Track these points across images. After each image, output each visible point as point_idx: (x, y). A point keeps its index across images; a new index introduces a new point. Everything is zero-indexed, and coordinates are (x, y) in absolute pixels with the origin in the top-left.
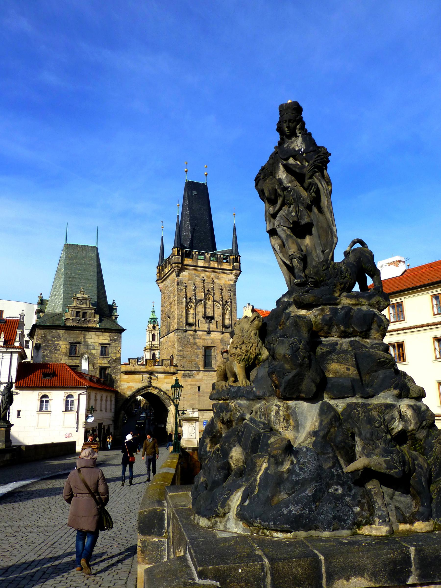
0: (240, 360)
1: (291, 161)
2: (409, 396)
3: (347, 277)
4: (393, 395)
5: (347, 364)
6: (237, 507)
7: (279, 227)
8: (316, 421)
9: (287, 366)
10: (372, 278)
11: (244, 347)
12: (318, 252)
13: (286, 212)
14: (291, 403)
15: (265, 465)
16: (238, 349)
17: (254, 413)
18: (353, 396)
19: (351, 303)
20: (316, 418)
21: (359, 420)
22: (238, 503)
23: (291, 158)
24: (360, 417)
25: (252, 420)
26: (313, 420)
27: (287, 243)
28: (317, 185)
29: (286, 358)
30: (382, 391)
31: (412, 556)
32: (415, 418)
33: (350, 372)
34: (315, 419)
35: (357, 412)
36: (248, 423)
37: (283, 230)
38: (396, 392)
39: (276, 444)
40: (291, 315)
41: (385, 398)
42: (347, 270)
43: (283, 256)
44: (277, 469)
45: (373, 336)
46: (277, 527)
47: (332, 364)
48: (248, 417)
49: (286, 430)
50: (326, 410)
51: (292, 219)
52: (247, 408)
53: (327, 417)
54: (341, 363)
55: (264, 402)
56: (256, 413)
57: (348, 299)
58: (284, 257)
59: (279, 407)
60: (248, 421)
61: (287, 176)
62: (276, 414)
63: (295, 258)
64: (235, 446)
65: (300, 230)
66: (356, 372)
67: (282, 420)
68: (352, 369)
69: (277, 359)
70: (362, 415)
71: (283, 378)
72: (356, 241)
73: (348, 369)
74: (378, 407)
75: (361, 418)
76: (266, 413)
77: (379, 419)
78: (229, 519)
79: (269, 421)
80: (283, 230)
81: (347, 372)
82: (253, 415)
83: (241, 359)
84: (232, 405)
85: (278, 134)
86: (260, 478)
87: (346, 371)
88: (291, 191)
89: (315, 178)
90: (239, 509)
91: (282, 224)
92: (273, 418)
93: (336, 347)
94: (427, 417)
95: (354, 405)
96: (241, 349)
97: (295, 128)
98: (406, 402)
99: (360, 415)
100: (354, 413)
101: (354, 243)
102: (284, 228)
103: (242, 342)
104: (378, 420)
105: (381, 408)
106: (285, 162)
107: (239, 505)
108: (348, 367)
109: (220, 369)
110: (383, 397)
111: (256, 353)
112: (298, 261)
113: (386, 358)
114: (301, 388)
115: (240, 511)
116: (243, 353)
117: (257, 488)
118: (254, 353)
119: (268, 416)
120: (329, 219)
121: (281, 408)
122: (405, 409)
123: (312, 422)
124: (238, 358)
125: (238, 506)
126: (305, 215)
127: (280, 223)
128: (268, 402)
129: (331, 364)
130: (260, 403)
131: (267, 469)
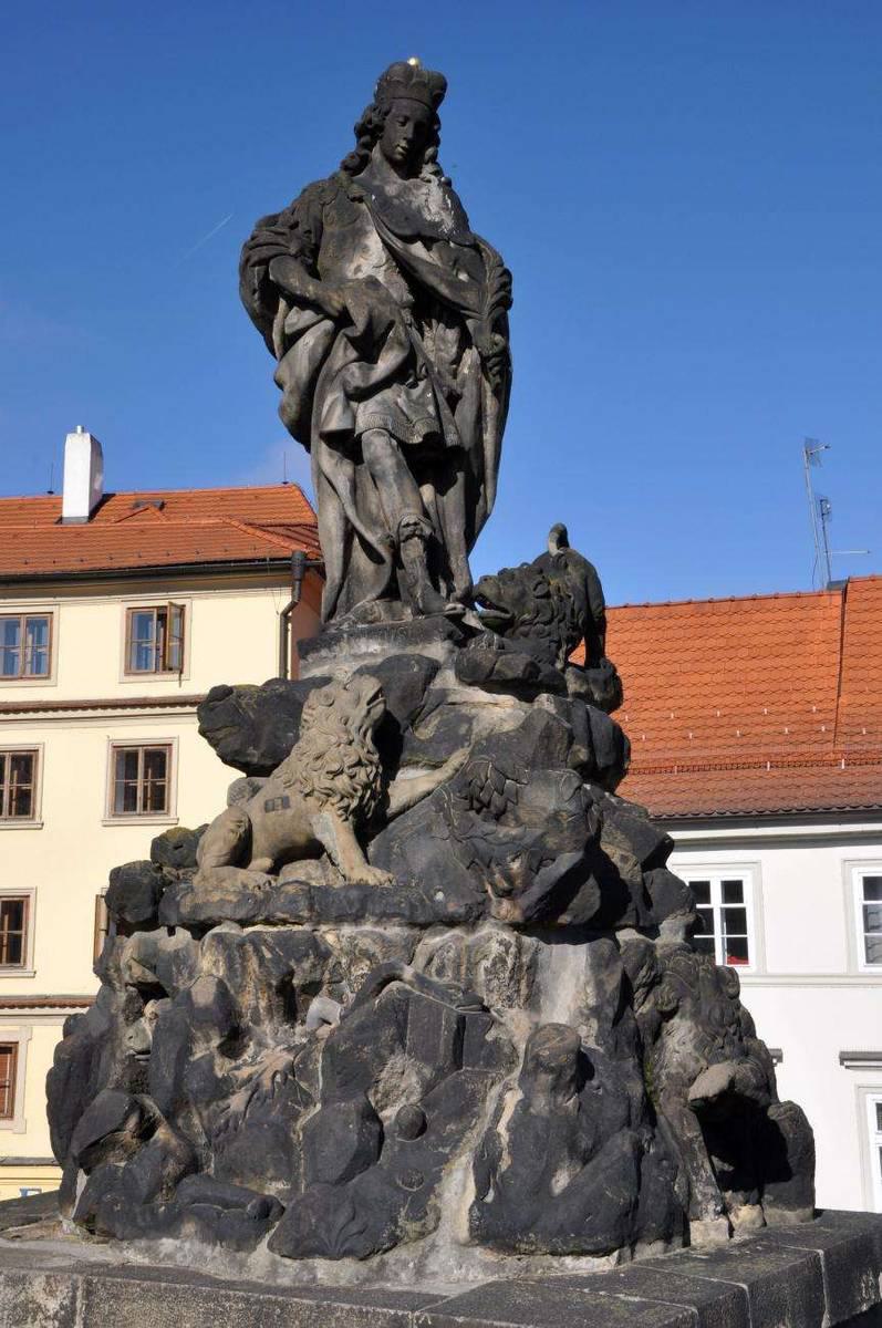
0: (346, 809)
6: (471, 1210)
8: (587, 983)
15: (512, 1099)
16: (344, 778)
17: (420, 961)
20: (586, 976)
21: (698, 978)
22: (471, 1196)
25: (421, 981)
26: (578, 979)
31: (822, 1263)
34: (582, 978)
36: (408, 987)
39: (549, 1040)
40: (450, 700)
44: (555, 1102)
46: (585, 1241)
49: (511, 1006)
58: (362, 522)
60: (410, 983)
62: (494, 964)
64: (392, 1052)
71: (537, 873)
78: (433, 1246)
79: (470, 984)
84: (330, 936)
86: (508, 1129)
90: (476, 1213)
92: (482, 976)
106: (398, 244)
107: (474, 1202)
115: (479, 1219)
116: (356, 790)
117: (505, 1155)
119: (468, 969)
125: (472, 1206)
130: (441, 933)
131: (525, 1105)
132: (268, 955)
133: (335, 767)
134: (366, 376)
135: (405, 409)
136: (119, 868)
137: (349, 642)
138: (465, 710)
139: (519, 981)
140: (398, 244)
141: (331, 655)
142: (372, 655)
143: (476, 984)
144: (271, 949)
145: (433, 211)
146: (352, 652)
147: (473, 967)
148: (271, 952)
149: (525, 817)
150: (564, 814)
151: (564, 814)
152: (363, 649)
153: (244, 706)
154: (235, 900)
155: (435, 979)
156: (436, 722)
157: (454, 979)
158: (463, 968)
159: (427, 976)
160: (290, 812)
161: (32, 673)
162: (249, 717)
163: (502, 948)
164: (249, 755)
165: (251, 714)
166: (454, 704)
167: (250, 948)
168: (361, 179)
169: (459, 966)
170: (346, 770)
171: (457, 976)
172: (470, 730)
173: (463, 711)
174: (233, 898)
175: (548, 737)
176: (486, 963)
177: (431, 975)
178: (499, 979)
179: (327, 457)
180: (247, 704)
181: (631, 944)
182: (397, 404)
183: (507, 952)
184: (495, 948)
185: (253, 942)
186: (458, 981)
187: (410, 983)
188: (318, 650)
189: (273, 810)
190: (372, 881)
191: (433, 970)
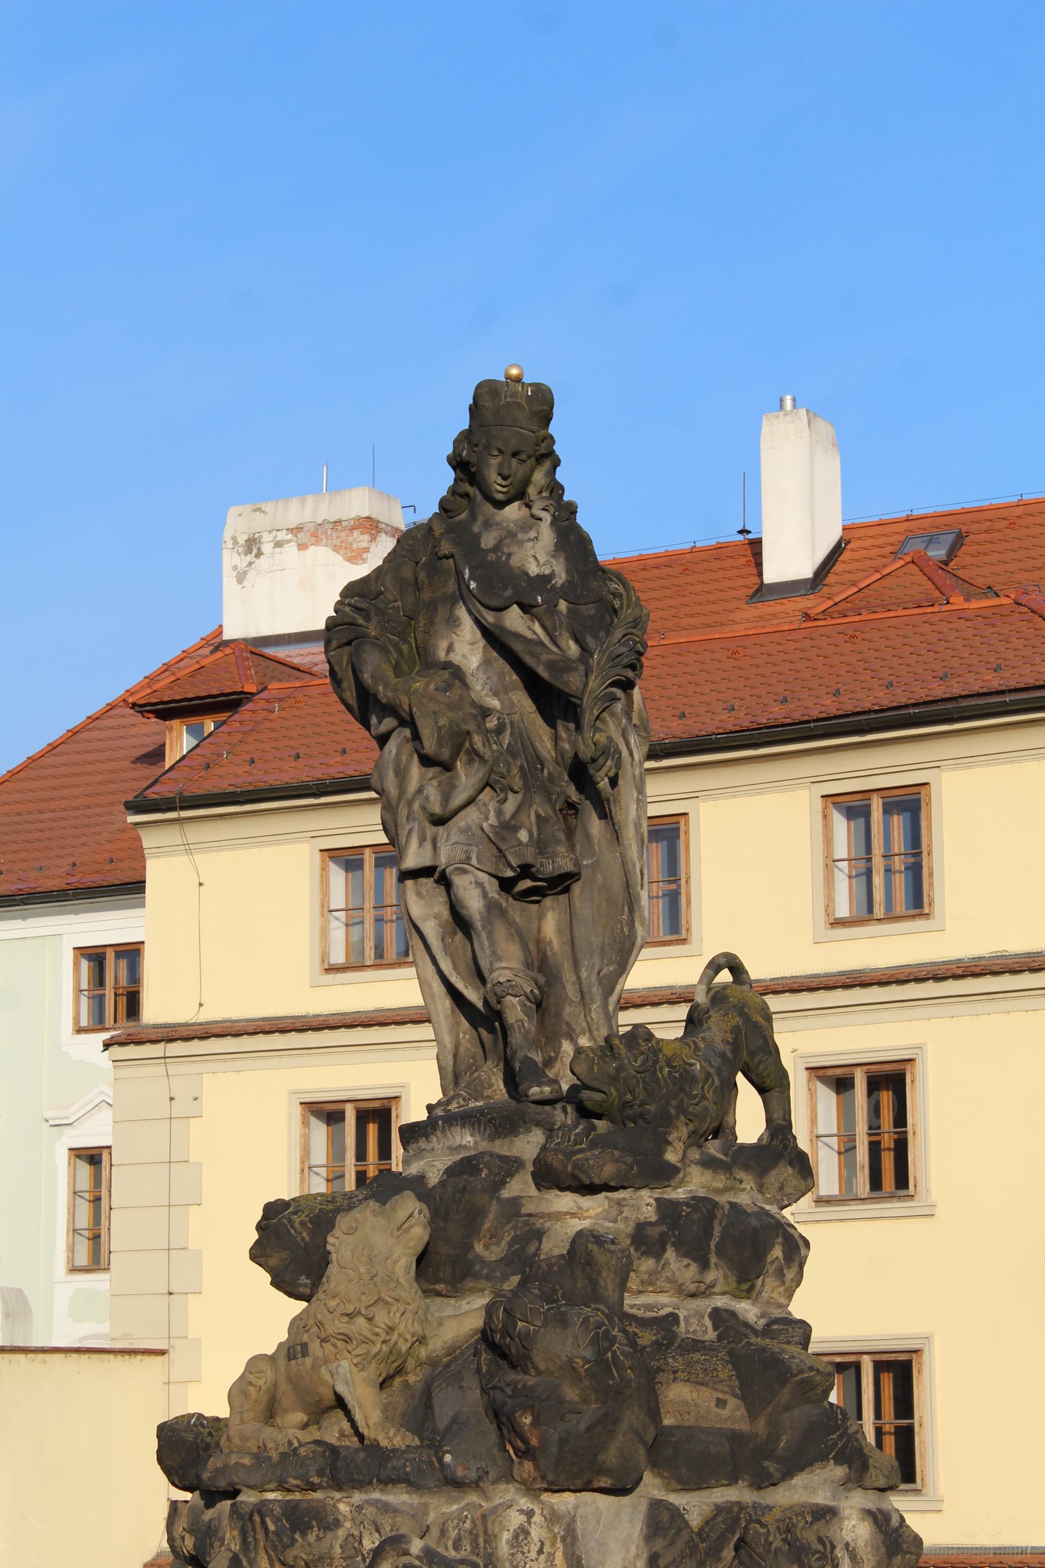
1: (514, 619)
2: (867, 1483)
3: (706, 1098)
4: (832, 1482)
5: (719, 1386)
7: (465, 872)
8: (637, 1557)
9: (571, 1393)
10: (762, 1090)
11: (382, 1318)
12: (584, 974)
13: (493, 820)
14: (565, 1501)
16: (361, 1321)
17: (435, 1533)
18: (733, 1481)
19: (715, 1184)
20: (638, 1547)
21: (769, 1551)
23: (515, 606)
24: (771, 1543)
26: (628, 1551)
27: (490, 936)
28: (620, 753)
29: (574, 1369)
30: (802, 1470)
32: (878, 1548)
33: (725, 1413)
34: (633, 1548)
35: (763, 1531)
36: (417, 1563)
37: (480, 885)
38: (841, 1472)
40: (523, 1211)
41: (813, 1486)
42: (708, 1075)
43: (455, 968)
45: (765, 1295)
47: (674, 1386)
48: (416, 1546)
50: (661, 1522)
51: (518, 855)
52: (413, 1516)
53: (672, 1543)
54: (702, 1384)
55: (474, 1498)
56: (443, 1533)
57: (706, 1172)
59: (530, 1514)
61: (486, 663)
62: (516, 1536)
63: (516, 996)
65: (530, 884)
66: (741, 1412)
67: (533, 1555)
68: (732, 1402)
69: (535, 1368)
70: (775, 1538)
72: (723, 961)
73: (721, 1403)
74: (796, 1515)
75: (773, 1546)
76: (482, 1533)
77: (820, 1547)
80: (480, 885)
81: (718, 1410)
82: (431, 1540)
83: (366, 1354)
85: (448, 476)
87: (715, 1409)
88: (499, 730)
89: (611, 723)
91: (474, 861)
93: (675, 1328)
94: (904, 1546)
95: (736, 1509)
96: (370, 1320)
97: (527, 481)
98: (856, 1499)
99: (771, 1539)
100: (756, 1532)
101: (714, 966)
102: (481, 874)
103: (376, 1298)
104: (817, 1552)
105: (804, 1517)
106: (490, 617)
108: (721, 1396)
109: (261, 1383)
110: (805, 1487)
111: (413, 1335)
112: (523, 1005)
113: (818, 1370)
114: (601, 1457)
116: (377, 1335)
118: (408, 1337)
119: (486, 1541)
120: (634, 866)
121: (537, 1518)
122: (853, 1522)
123: (624, 1559)
124: (359, 1351)
126: (558, 842)
127: (469, 858)
128: (487, 1498)
129: (668, 1385)
132: (272, 1527)
133: (350, 1309)
134: (446, 798)
135: (491, 835)
136: (165, 1423)
137: (443, 1131)
138: (538, 1223)
139: (551, 1556)
140: (490, 617)
141: (429, 1147)
142: (465, 1147)
143: (498, 1560)
144: (277, 1520)
145: (542, 561)
146: (448, 1144)
147: (490, 1539)
148: (276, 1525)
149: (542, 1366)
150: (578, 1360)
151: (579, 1361)
152: (458, 1141)
153: (297, 1225)
154: (249, 1464)
155: (452, 1554)
156: (508, 1239)
157: (472, 1552)
158: (481, 1540)
159: (441, 1550)
160: (308, 1361)
161: (665, 934)
162: (303, 1239)
163: (523, 1518)
164: (300, 1285)
165: (305, 1234)
166: (530, 1215)
167: (257, 1518)
168: (461, 521)
169: (477, 1537)
170: (363, 1312)
171: (475, 1546)
172: (538, 1249)
173: (538, 1225)
174: (247, 1461)
175: (589, 1265)
176: (506, 1536)
177: (447, 1549)
178: (523, 1553)
179: (414, 897)
180: (302, 1223)
181: (723, 1508)
182: (482, 829)
183: (529, 1523)
184: (516, 1519)
185: (259, 1512)
186: (478, 1555)
187: (418, 1557)
188: (417, 1141)
189: (295, 1358)
190: (384, 1443)
191: (450, 1543)
